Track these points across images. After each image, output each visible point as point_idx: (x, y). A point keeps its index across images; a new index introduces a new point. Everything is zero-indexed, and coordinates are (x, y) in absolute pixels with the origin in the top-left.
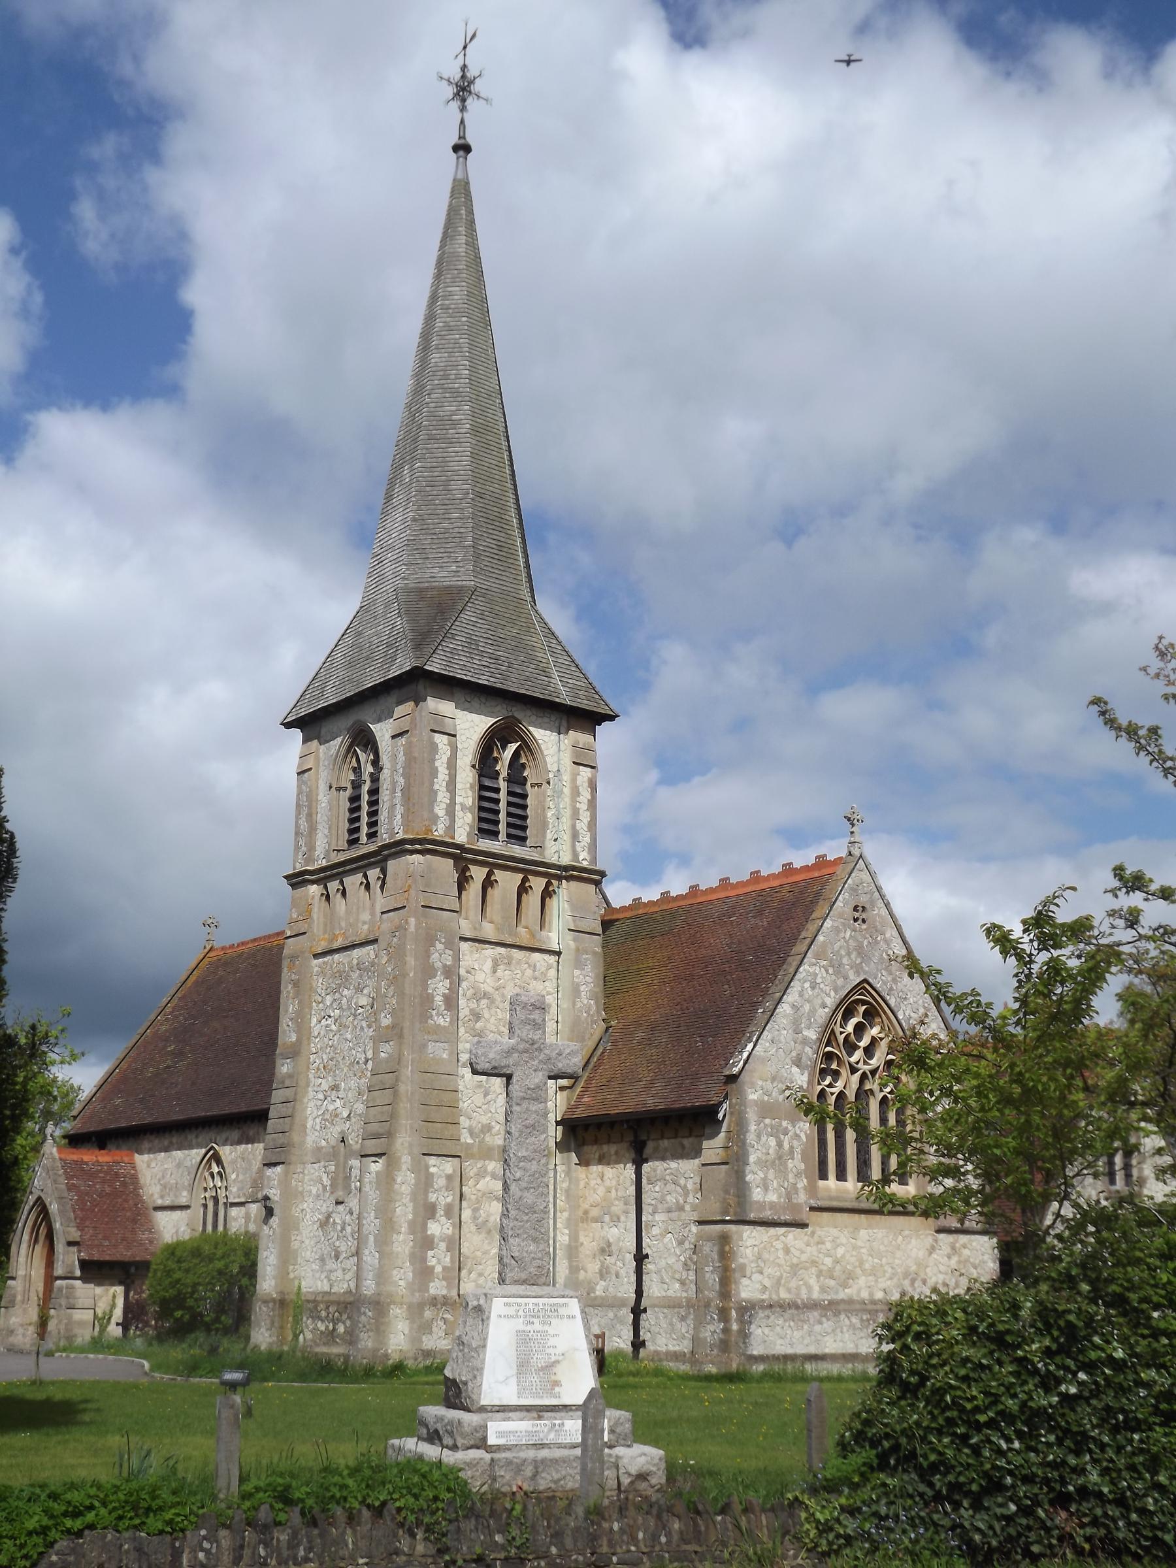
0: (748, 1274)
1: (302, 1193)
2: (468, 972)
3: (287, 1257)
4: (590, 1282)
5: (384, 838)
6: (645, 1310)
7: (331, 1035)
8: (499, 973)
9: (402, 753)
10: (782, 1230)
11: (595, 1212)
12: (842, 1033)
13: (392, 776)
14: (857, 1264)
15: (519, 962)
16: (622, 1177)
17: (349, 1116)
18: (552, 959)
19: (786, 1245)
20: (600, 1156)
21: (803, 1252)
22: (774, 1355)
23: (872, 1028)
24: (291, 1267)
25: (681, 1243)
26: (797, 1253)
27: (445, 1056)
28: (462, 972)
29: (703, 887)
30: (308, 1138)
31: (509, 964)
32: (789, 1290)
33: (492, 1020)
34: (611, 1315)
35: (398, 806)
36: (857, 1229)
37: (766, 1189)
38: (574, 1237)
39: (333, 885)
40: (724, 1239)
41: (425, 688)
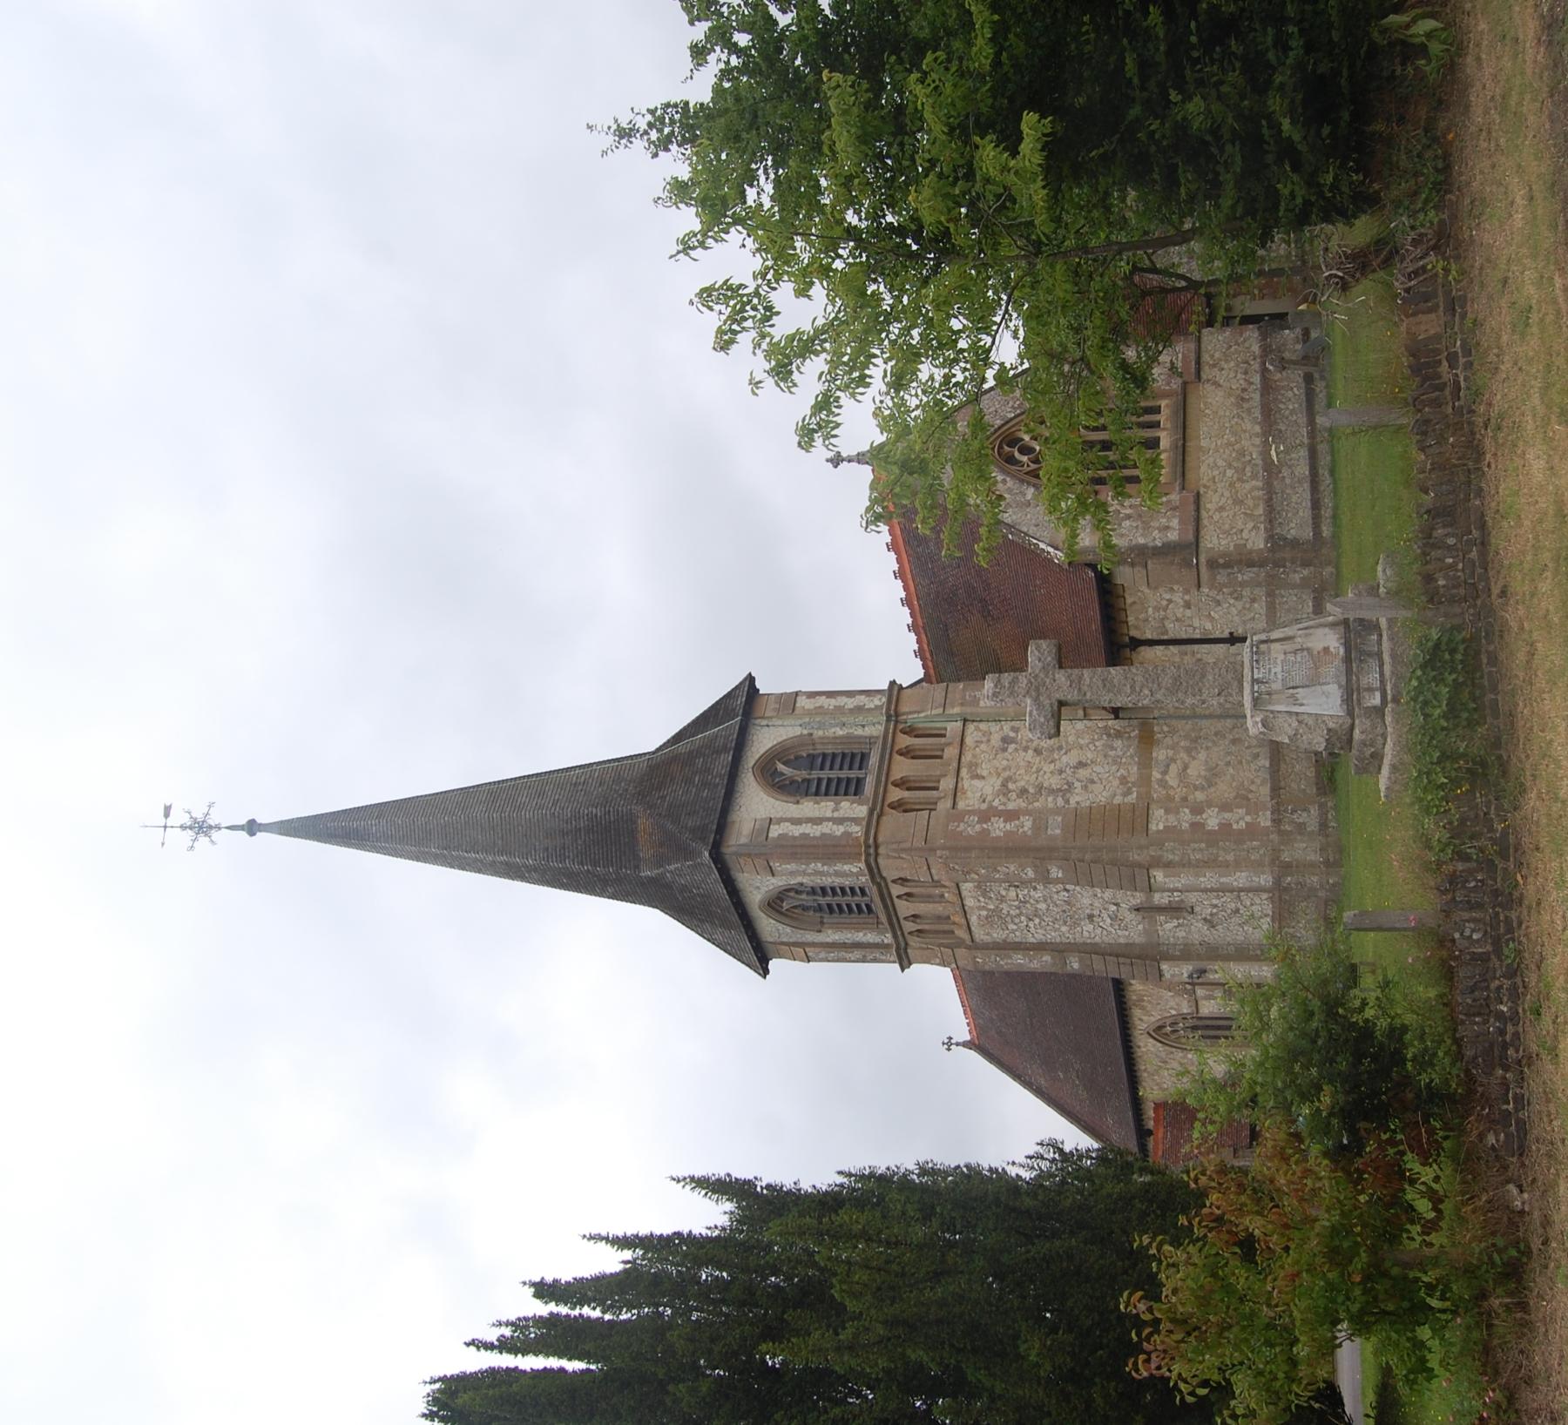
0: (1243, 542)
1: (1185, 945)
2: (984, 801)
3: (1243, 954)
5: (864, 879)
7: (1043, 923)
8: (985, 773)
9: (788, 866)
10: (1204, 514)
12: (1028, 466)
13: (809, 875)
14: (1231, 448)
15: (974, 756)
17: (1114, 904)
18: (971, 727)
19: (1216, 510)
21: (1222, 495)
22: (1313, 519)
23: (1023, 440)
24: (1251, 953)
25: (1218, 603)
26: (1223, 500)
27: (1060, 819)
28: (984, 806)
29: (903, 595)
30: (1137, 941)
31: (976, 765)
32: (1255, 506)
33: (1027, 778)
36: (1200, 448)
37: (1167, 528)
39: (909, 926)
40: (1213, 564)
41: (728, 846)
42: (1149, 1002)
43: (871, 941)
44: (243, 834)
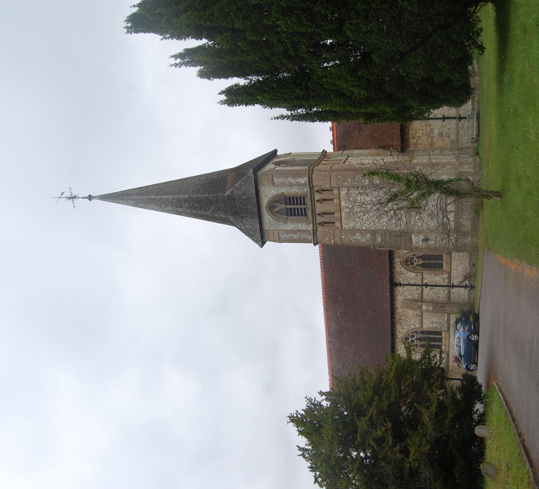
4: (451, 142)
6: (460, 115)
11: (430, 140)
16: (420, 128)
20: (413, 138)
34: (461, 131)
35: (297, 181)
38: (437, 149)
42: (404, 320)
43: (304, 229)
44: (87, 200)
